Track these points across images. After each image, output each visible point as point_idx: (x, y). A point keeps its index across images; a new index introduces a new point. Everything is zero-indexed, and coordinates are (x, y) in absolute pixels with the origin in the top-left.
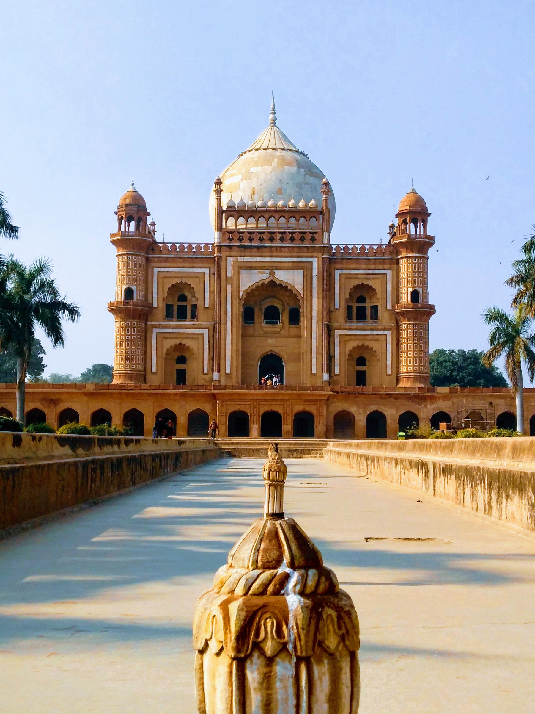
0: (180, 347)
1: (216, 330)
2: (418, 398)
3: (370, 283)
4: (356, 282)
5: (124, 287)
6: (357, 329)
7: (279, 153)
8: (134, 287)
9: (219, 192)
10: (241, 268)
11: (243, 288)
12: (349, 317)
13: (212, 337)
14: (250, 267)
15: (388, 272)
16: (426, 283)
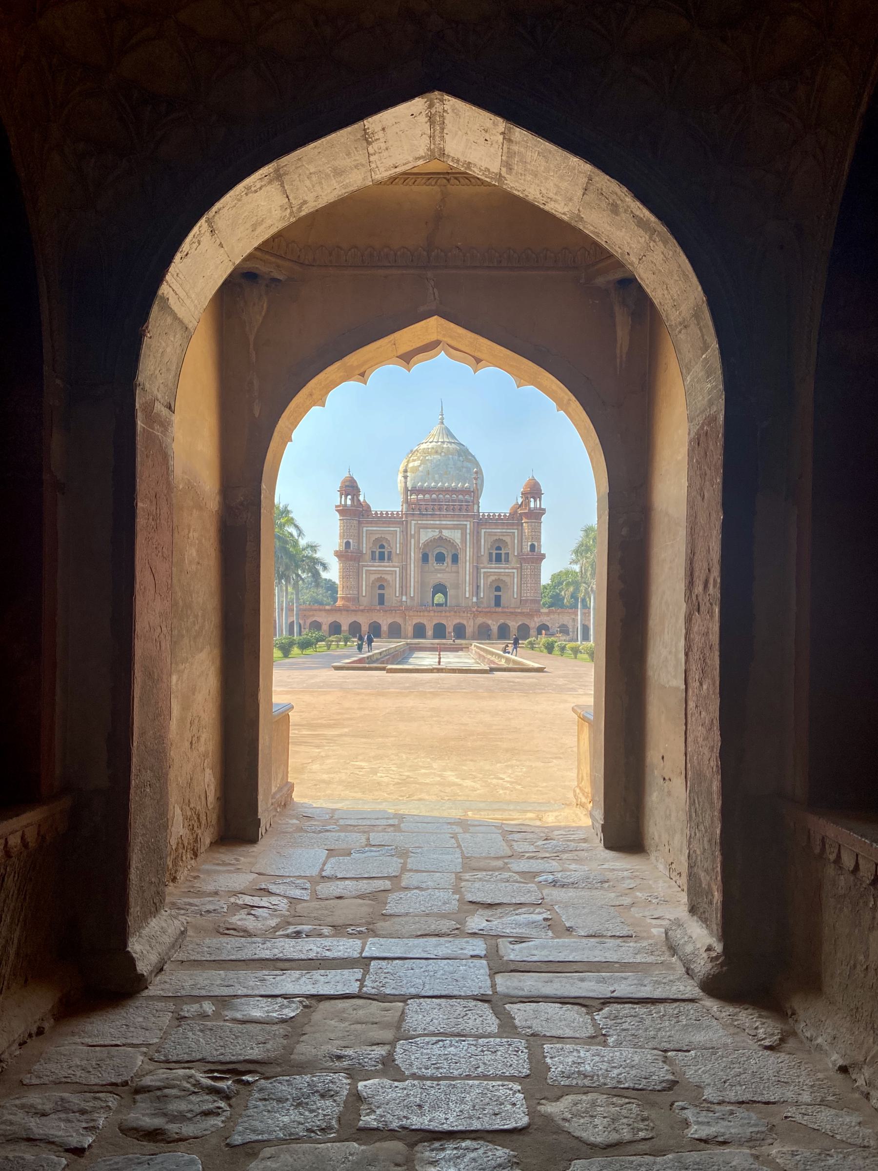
0: (381, 579)
1: (404, 569)
2: (530, 615)
3: (504, 538)
4: (495, 538)
5: (345, 541)
6: (496, 568)
7: (445, 446)
8: (351, 541)
9: (406, 477)
10: (420, 528)
11: (421, 542)
12: (490, 560)
13: (401, 573)
14: (426, 527)
15: (516, 531)
16: (540, 539)
